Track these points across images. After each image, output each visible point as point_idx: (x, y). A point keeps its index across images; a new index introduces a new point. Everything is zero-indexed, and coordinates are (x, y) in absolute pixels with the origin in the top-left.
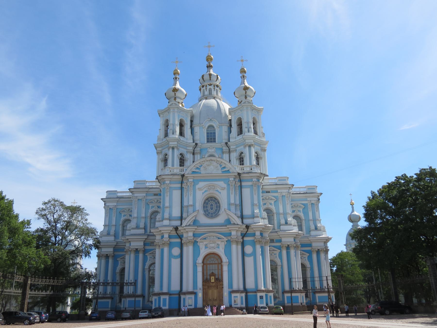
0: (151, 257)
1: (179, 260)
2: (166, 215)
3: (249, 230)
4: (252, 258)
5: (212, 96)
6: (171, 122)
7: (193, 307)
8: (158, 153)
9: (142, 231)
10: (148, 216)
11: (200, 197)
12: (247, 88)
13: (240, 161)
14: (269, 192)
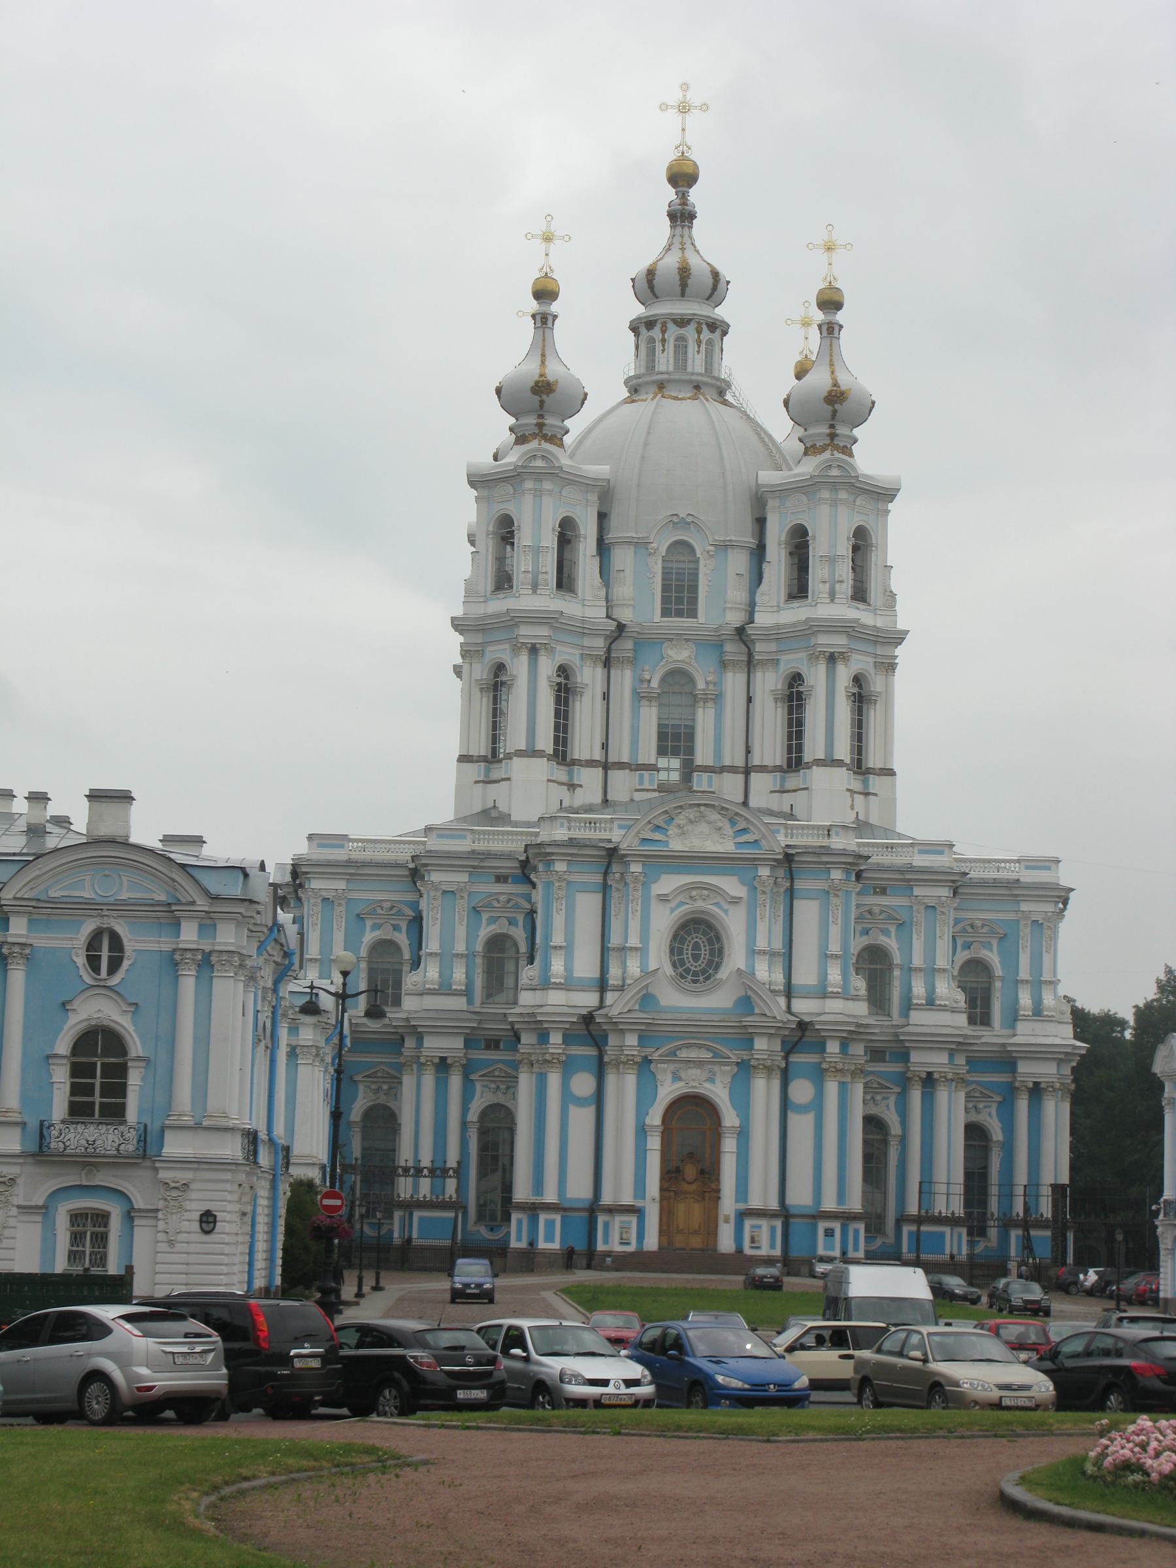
0: (487, 1086)
3: (808, 1034)
4: (808, 1119)
5: (687, 378)
6: (524, 537)
7: (631, 1248)
9: (460, 1003)
10: (477, 950)
11: (663, 921)
12: (842, 393)
13: (790, 709)
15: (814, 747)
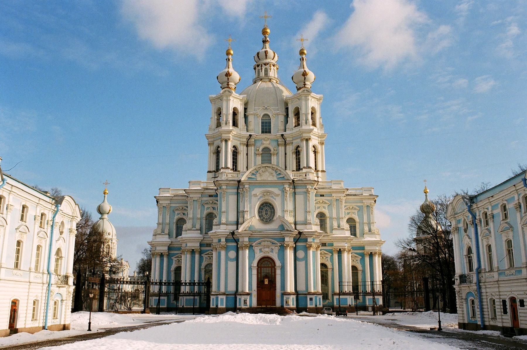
1: (235, 262)
2: (224, 220)
8: (209, 144)
13: (296, 155)
14: (323, 196)
15: (303, 164)
